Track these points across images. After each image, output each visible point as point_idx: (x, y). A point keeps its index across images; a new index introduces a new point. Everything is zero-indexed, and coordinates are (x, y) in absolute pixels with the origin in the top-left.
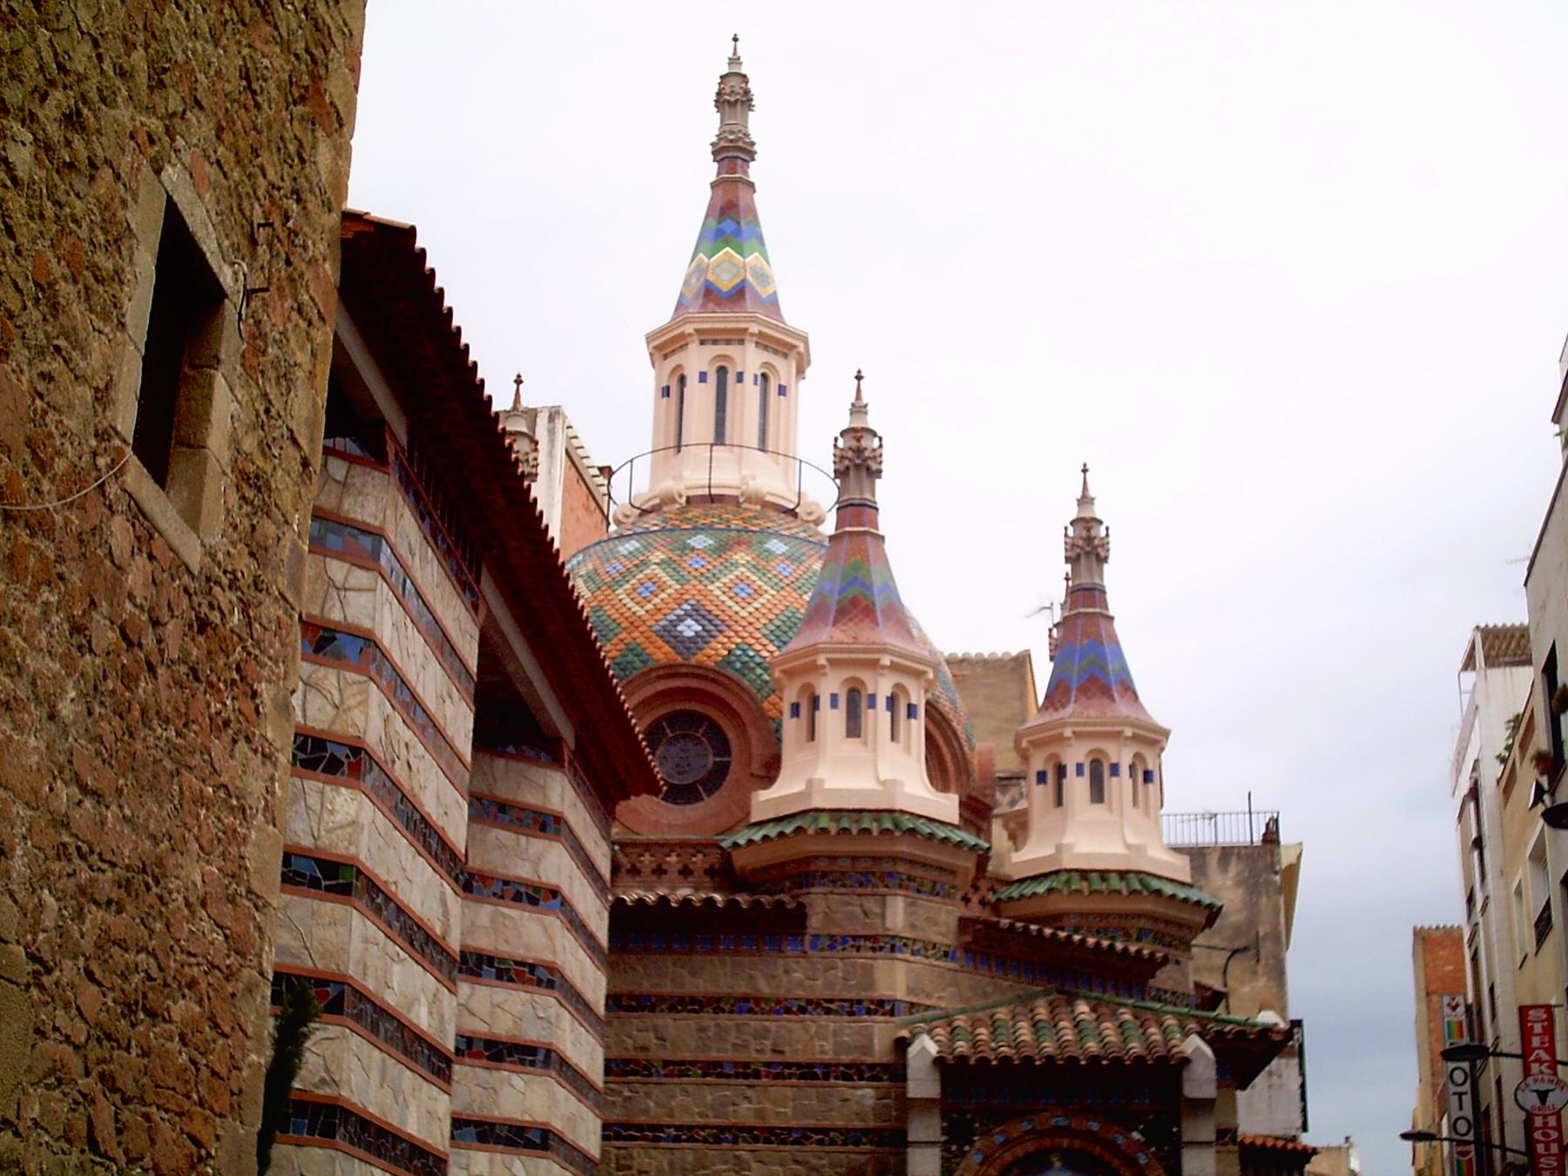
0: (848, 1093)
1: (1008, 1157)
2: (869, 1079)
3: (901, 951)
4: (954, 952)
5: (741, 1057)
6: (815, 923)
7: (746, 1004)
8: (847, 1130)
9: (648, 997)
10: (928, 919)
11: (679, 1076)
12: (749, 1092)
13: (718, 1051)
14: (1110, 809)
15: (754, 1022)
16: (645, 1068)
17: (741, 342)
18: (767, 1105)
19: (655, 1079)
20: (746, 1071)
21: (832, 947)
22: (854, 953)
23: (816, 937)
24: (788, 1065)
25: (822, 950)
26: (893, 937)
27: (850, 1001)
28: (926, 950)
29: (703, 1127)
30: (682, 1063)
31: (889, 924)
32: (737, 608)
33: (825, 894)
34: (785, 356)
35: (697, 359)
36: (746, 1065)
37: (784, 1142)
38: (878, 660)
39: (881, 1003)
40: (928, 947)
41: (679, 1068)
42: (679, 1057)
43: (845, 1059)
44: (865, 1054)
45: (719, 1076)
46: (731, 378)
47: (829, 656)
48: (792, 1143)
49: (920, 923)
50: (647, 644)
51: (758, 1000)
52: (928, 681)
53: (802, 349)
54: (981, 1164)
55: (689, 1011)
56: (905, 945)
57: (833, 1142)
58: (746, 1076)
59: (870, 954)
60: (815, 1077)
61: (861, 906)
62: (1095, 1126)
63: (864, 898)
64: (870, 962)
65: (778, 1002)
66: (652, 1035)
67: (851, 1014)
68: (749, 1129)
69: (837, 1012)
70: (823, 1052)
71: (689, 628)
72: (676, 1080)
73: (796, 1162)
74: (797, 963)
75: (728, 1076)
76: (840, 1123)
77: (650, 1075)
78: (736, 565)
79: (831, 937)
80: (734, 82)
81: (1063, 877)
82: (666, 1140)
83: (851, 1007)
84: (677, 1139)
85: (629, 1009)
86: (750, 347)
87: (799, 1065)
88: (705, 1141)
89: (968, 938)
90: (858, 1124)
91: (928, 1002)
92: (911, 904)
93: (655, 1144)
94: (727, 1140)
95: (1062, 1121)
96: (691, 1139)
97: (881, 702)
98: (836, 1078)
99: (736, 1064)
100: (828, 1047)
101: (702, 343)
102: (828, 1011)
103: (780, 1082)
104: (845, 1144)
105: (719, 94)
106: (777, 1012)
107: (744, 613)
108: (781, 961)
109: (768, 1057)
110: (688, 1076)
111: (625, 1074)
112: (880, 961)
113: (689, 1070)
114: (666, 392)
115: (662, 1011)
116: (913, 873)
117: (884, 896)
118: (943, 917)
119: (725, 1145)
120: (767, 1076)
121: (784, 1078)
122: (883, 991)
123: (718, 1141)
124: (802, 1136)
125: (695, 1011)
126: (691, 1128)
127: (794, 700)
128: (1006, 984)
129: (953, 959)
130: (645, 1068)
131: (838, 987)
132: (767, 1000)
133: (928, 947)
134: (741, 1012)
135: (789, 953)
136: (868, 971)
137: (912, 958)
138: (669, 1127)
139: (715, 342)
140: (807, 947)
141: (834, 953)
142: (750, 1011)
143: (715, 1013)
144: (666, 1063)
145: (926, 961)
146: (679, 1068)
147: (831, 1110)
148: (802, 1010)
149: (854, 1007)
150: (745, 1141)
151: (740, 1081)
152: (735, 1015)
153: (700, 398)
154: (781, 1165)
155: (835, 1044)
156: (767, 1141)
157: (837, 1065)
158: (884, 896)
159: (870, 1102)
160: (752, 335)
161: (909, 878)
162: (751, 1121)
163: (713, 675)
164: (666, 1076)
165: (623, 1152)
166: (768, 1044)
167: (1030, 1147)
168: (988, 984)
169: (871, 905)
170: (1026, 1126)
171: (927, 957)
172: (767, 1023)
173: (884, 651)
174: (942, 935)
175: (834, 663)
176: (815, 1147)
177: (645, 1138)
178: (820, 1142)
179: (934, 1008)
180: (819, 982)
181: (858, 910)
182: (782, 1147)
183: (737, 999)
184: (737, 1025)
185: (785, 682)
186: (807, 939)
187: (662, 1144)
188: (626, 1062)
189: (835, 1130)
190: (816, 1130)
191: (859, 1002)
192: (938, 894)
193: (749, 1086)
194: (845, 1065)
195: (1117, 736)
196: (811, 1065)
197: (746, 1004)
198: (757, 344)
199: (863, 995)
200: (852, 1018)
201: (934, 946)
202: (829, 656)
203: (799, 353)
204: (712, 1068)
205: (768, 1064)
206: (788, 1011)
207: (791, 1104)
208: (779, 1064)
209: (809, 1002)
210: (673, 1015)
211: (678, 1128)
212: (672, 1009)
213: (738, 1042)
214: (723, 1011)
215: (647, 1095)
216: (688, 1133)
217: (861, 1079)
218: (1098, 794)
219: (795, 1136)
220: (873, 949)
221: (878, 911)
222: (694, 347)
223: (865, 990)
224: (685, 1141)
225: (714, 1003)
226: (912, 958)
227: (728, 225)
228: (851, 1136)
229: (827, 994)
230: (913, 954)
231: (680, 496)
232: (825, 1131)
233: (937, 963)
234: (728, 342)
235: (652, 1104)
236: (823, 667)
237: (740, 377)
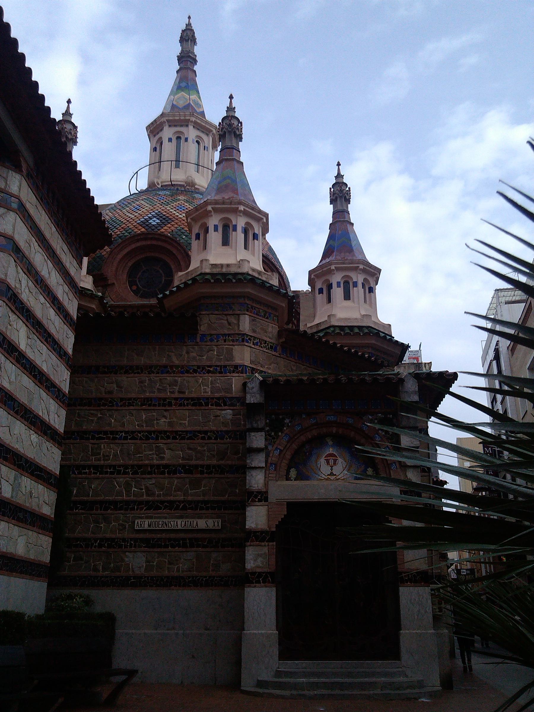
0: (218, 413)
1: (303, 438)
2: (229, 405)
3: (248, 342)
4: (276, 348)
5: (162, 395)
6: (203, 328)
7: (165, 369)
8: (218, 431)
10: (262, 329)
11: (128, 406)
12: (166, 414)
13: (150, 392)
14: (354, 301)
15: (169, 379)
16: (110, 402)
17: (187, 126)
18: (175, 420)
19: (115, 408)
20: (165, 403)
23: (203, 335)
24: (187, 399)
25: (206, 342)
26: (244, 334)
27: (220, 366)
28: (261, 344)
29: (139, 432)
30: (130, 399)
31: (241, 328)
32: (178, 214)
33: (208, 314)
35: (168, 133)
36: (165, 399)
37: (183, 438)
38: (238, 208)
39: (236, 367)
40: (261, 342)
41: (128, 402)
42: (129, 396)
43: (217, 395)
44: (228, 393)
45: (150, 405)
46: (183, 140)
47: (213, 206)
48: (188, 439)
49: (258, 330)
50: (134, 228)
51: (172, 367)
52: (263, 223)
54: (288, 442)
55: (135, 373)
56: (249, 339)
57: (210, 438)
58: (164, 405)
60: (200, 404)
61: (227, 320)
62: (351, 421)
63: (229, 317)
64: (231, 347)
65: (182, 367)
66: (115, 386)
67: (220, 373)
68: (165, 432)
69: (213, 372)
70: (205, 392)
71: (154, 222)
72: (127, 408)
73: (189, 449)
74: (193, 348)
75: (155, 405)
76: (214, 428)
77: (113, 406)
78: (179, 200)
79: (211, 335)
80: (189, 32)
81: (332, 329)
82: (120, 439)
83: (221, 369)
84: (126, 438)
85: (105, 373)
86: (191, 127)
87: (193, 399)
88: (141, 439)
89: (284, 340)
90: (225, 429)
91: (261, 369)
92: (253, 320)
93: (113, 441)
94: (152, 438)
95: (332, 418)
96: (133, 438)
97: (239, 229)
98: (212, 405)
99: (160, 399)
100: (208, 390)
101: (170, 126)
102: (209, 372)
103: (182, 408)
104: (216, 439)
105: (181, 37)
106: (182, 373)
107: (180, 216)
108: (185, 348)
109: (176, 395)
110: (133, 406)
111: (99, 405)
113: (133, 402)
114: (155, 149)
116: (254, 305)
117: (239, 315)
118: (270, 329)
119: (151, 441)
120: (175, 405)
121: (184, 406)
122: (238, 361)
123: (147, 438)
124: (193, 435)
125: (138, 373)
126: (133, 432)
127: (197, 231)
128: (303, 367)
129: (275, 350)
130: (110, 402)
131: (214, 360)
132: (177, 367)
133: (261, 342)
134: (162, 373)
136: (230, 352)
137: (253, 346)
138: (121, 432)
139: (175, 126)
140: (198, 340)
142: (168, 372)
143: (149, 373)
144: (122, 399)
145: (261, 349)
146: (128, 402)
147: (209, 421)
148: (195, 371)
149: (222, 370)
150: (162, 438)
151: (161, 408)
152: (160, 375)
153: (169, 150)
154: (182, 451)
155: (211, 388)
156: (174, 438)
157: (213, 398)
158: (239, 315)
159: (230, 417)
160: (192, 121)
161: (252, 307)
162: (166, 428)
163: (163, 238)
164: (121, 406)
165: (96, 446)
166: (177, 388)
167: (315, 433)
168: (294, 366)
169: (233, 320)
170: (312, 421)
171: (262, 347)
172: (176, 378)
173: (240, 203)
175: (216, 210)
176: (200, 441)
177: (108, 438)
178: (203, 438)
179: (265, 372)
180: (205, 357)
181: (226, 322)
182: (183, 441)
183: (160, 366)
184: (160, 379)
185: (193, 223)
187: (117, 441)
188: (100, 399)
189: (211, 432)
190: (200, 432)
191: (225, 367)
192: (267, 318)
193: (166, 410)
194: (216, 398)
195: (356, 269)
196: (199, 399)
197: (165, 369)
198: (194, 127)
199: (227, 363)
200: (222, 375)
201: (266, 341)
202: (213, 206)
203: (213, 134)
204: (147, 402)
205: (176, 399)
206: (188, 372)
207: (188, 419)
208: (183, 398)
209: (199, 367)
211: (126, 432)
212: (126, 372)
213: (160, 388)
214: (154, 373)
215: (111, 416)
216: (132, 435)
217: (225, 405)
219: (189, 435)
220: (233, 341)
221: (235, 322)
222: (166, 128)
223: (228, 361)
224: (130, 439)
225: (150, 369)
226: (253, 346)
227: (183, 84)
228: (219, 435)
229: (208, 363)
230: (254, 344)
231: (158, 184)
232: (206, 432)
233: (266, 351)
234: (182, 126)
235: (113, 421)
236: (210, 211)
237: (186, 140)
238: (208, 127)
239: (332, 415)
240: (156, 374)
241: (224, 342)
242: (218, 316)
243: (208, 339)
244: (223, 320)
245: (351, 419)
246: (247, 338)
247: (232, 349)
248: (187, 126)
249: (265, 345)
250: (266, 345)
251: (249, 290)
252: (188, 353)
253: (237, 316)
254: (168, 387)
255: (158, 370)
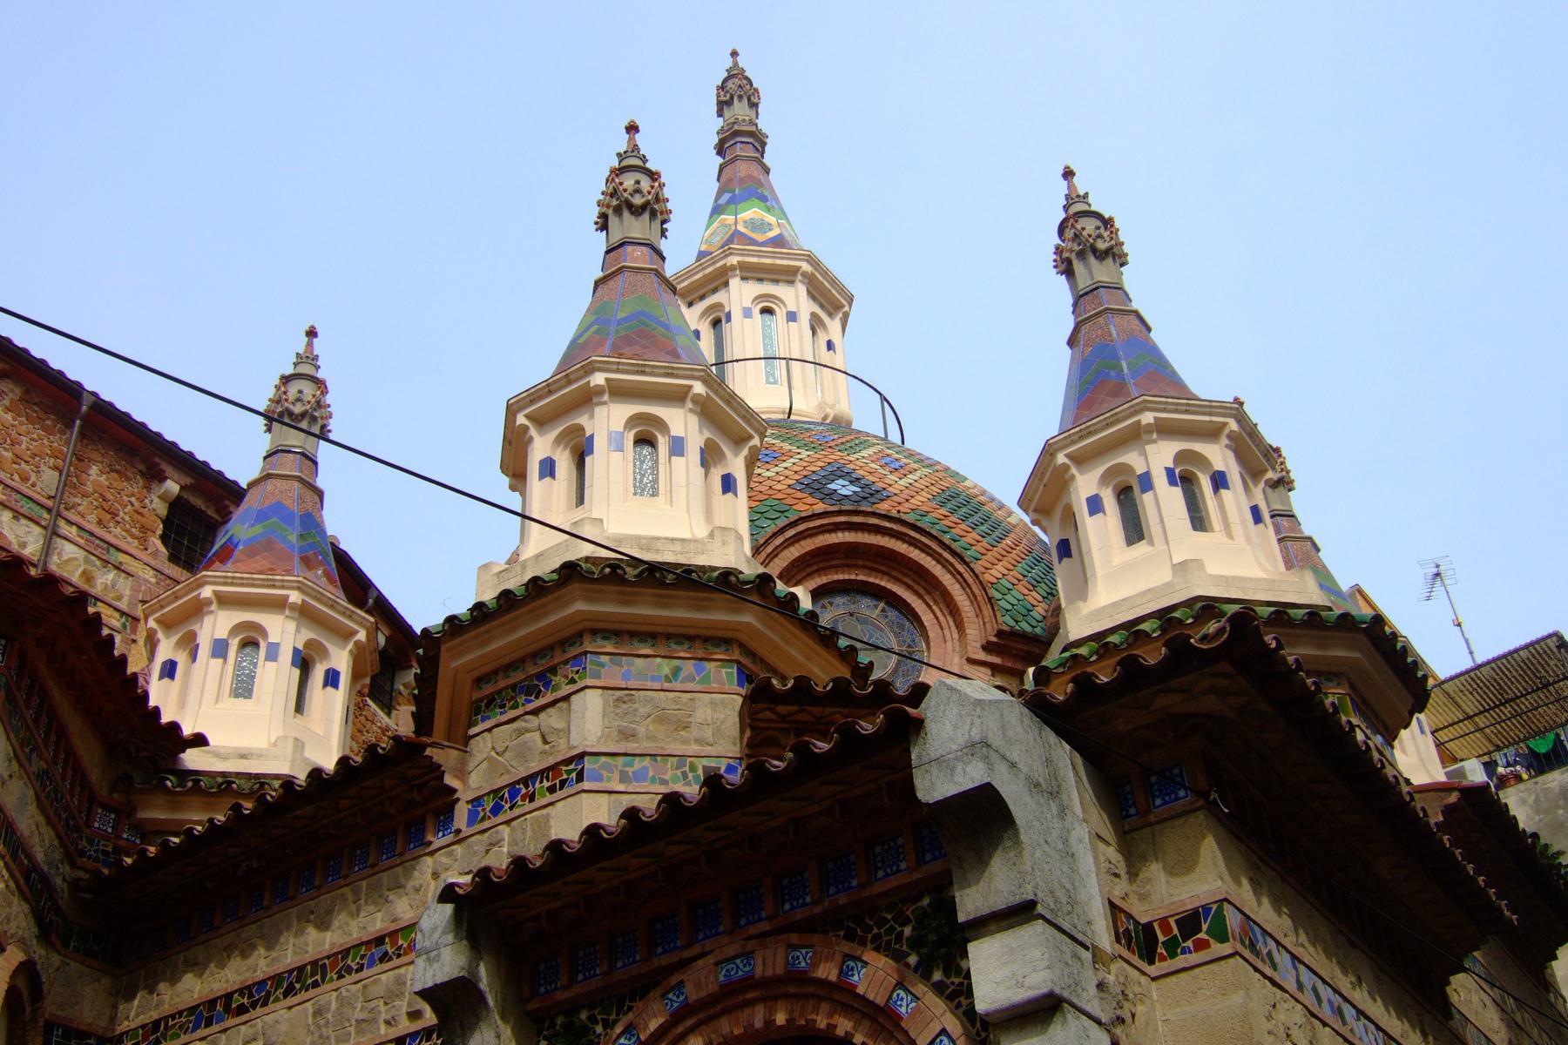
9: (262, 983)
10: (662, 720)
14: (1151, 543)
21: (496, 810)
22: (529, 806)
23: (476, 801)
25: (483, 819)
31: (575, 739)
33: (489, 730)
34: (791, 282)
53: (806, 267)
59: (549, 798)
63: (543, 715)
64: (544, 811)
74: (450, 854)
85: (242, 1010)
112: (559, 805)
115: (277, 1000)
117: (567, 698)
125: (316, 985)
135: (437, 843)
137: (621, 787)
141: (501, 818)
158: (567, 698)
160: (733, 268)
169: (551, 719)
172: (402, 970)
174: (698, 741)
181: (537, 736)
186: (461, 812)
203: (805, 275)
210: (291, 1001)
214: (349, 970)
218: (1134, 530)
220: (552, 790)
230: (624, 778)
238: (785, 262)
239: (737, 956)
240: (357, 971)
241: (530, 802)
242: (515, 725)
243: (488, 809)
244: (528, 731)
245: (804, 951)
246: (596, 766)
247: (547, 818)
248: (726, 284)
249: (679, 772)
250: (687, 769)
251: (581, 606)
252: (436, 875)
253: (563, 705)
254: (383, 1008)
255: (363, 957)
